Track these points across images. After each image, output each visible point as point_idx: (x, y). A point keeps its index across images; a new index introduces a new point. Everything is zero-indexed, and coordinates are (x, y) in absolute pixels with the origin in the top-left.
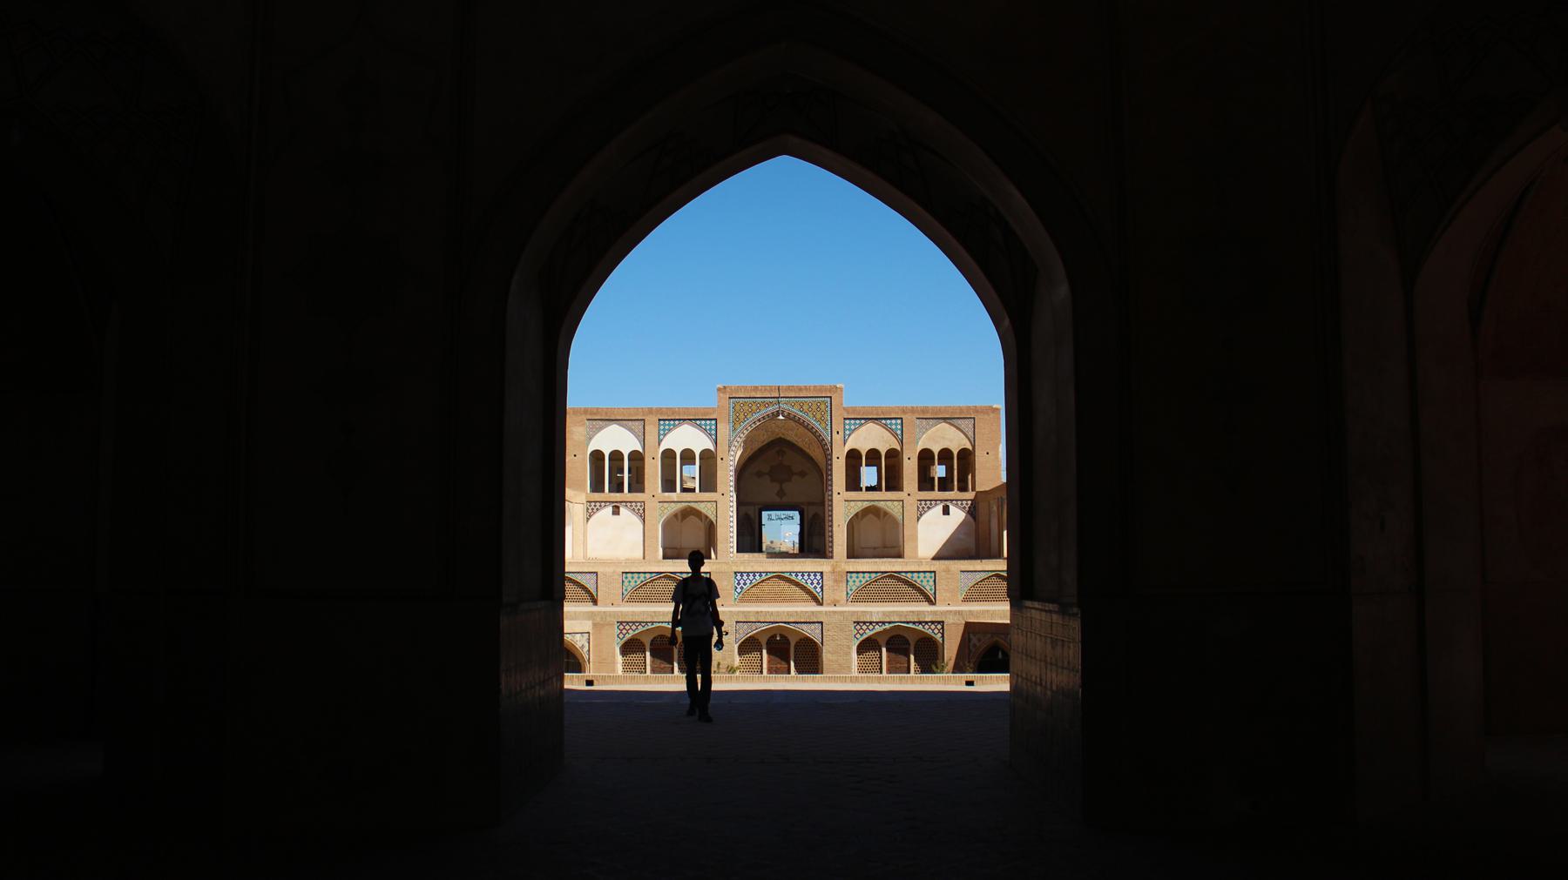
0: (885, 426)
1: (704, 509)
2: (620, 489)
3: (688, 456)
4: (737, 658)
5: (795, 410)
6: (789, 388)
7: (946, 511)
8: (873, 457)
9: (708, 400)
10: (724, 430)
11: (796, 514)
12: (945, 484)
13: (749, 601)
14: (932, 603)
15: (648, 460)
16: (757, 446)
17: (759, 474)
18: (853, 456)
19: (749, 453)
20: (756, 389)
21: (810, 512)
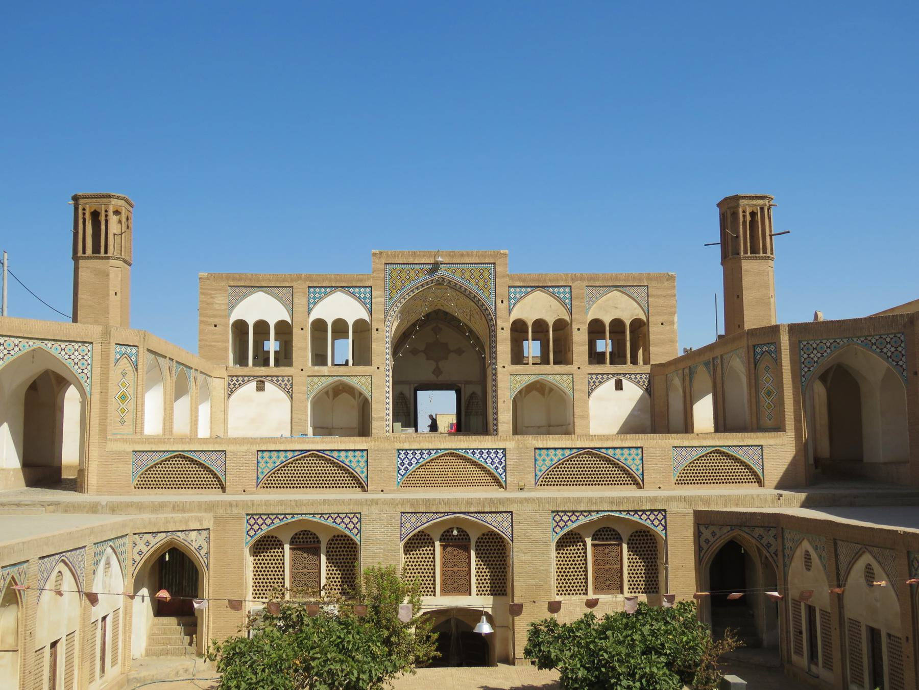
0: (553, 295)
1: (358, 383)
3: (340, 328)
4: (403, 559)
5: (457, 278)
7: (619, 386)
8: (540, 327)
10: (379, 298)
12: (617, 357)
13: (415, 486)
14: (640, 486)
15: (296, 331)
16: (413, 318)
17: (415, 352)
18: (519, 329)
19: (406, 325)
20: (414, 254)
21: (467, 391)
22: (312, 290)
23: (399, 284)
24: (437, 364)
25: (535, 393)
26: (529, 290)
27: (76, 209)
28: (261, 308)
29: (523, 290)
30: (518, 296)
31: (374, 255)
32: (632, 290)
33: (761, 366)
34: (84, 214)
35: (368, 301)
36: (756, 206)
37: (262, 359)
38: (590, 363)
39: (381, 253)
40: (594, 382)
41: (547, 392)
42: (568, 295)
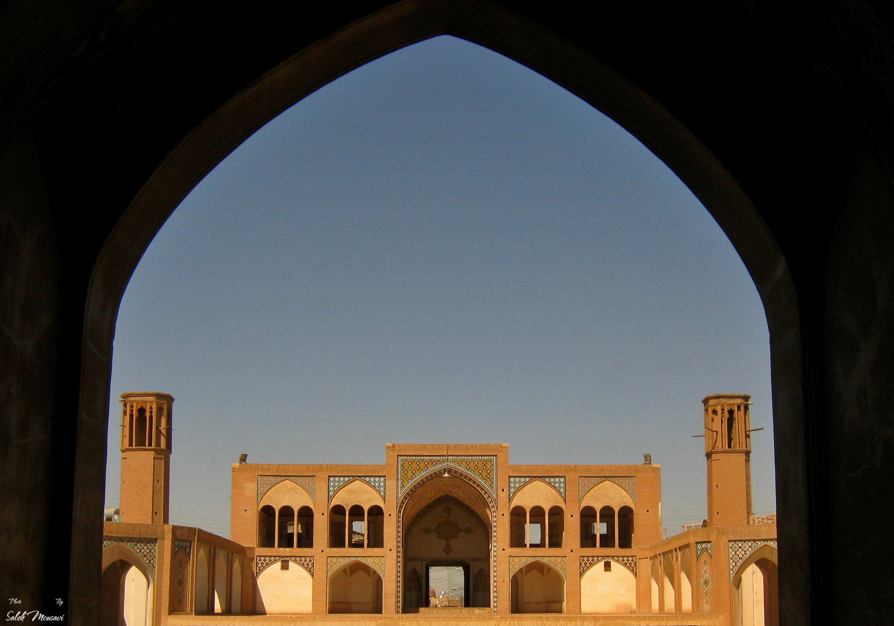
0: (549, 484)
2: (290, 545)
3: (357, 512)
5: (462, 469)
6: (456, 447)
7: (607, 567)
8: (537, 514)
9: (377, 457)
10: (391, 485)
11: (461, 568)
12: (607, 541)
17: (427, 531)
18: (518, 515)
20: (424, 447)
21: (475, 568)
22: (332, 479)
23: (410, 474)
24: (448, 542)
25: (534, 571)
26: (527, 479)
27: (125, 405)
28: (289, 496)
29: (522, 480)
30: (517, 485)
31: (388, 447)
32: (620, 480)
33: (702, 559)
34: (132, 411)
35: (382, 489)
36: (734, 405)
37: (287, 541)
38: (583, 545)
39: (394, 446)
40: (585, 564)
41: (545, 571)
42: (562, 485)
